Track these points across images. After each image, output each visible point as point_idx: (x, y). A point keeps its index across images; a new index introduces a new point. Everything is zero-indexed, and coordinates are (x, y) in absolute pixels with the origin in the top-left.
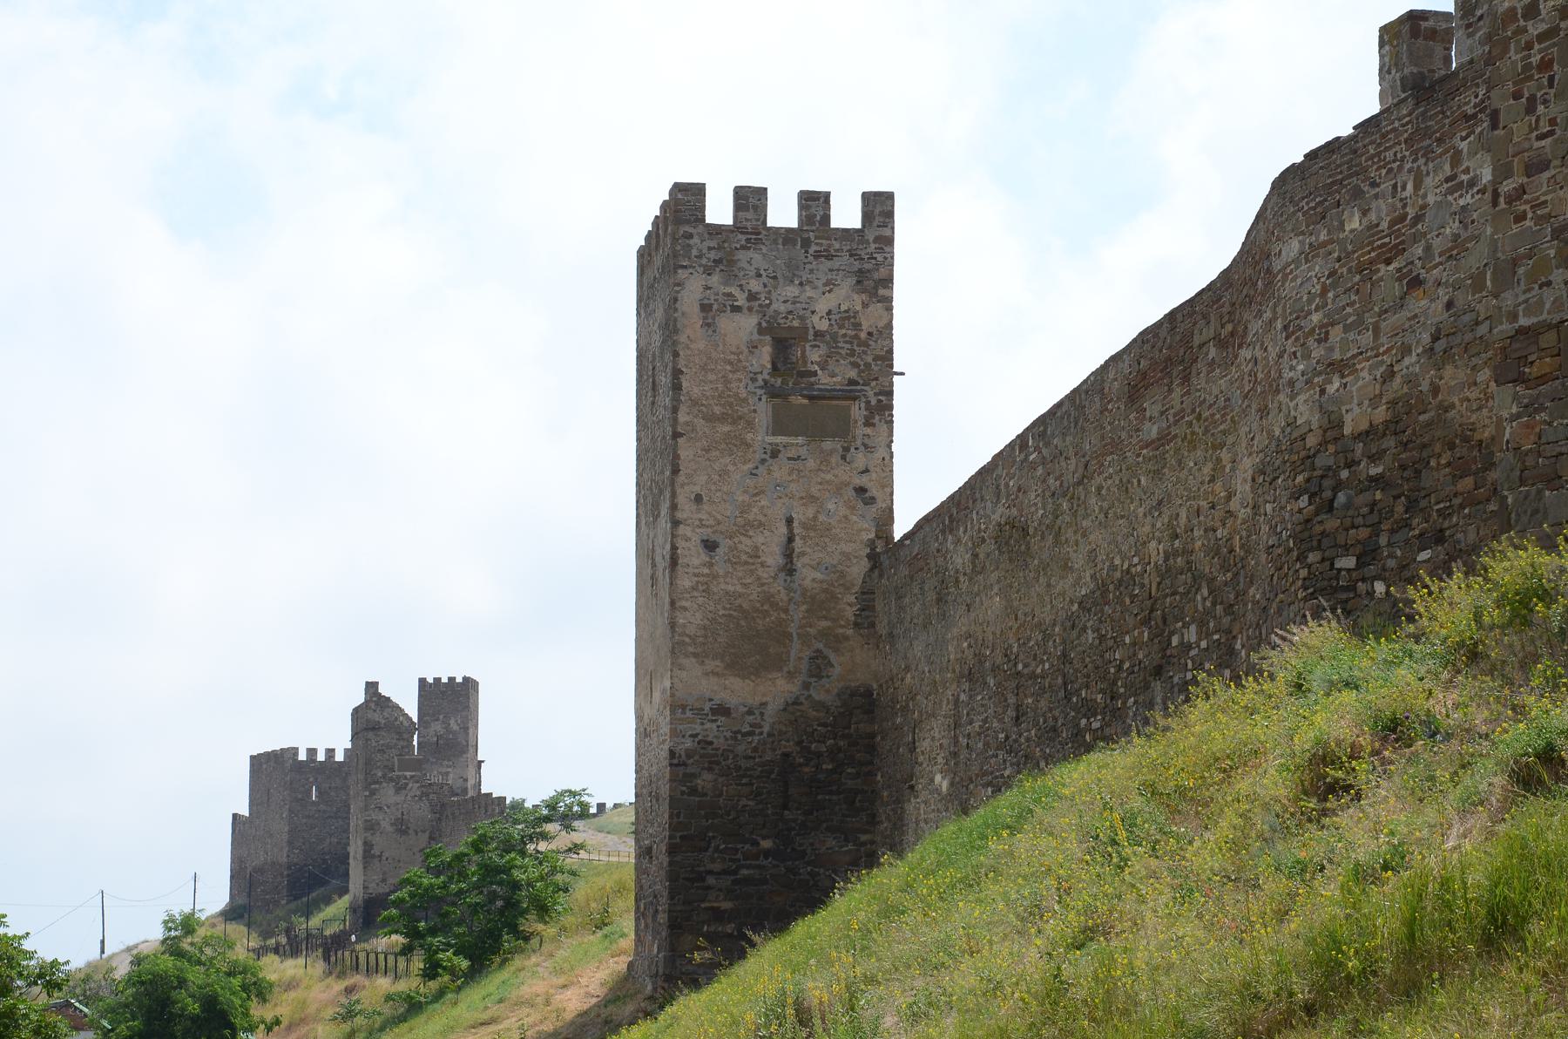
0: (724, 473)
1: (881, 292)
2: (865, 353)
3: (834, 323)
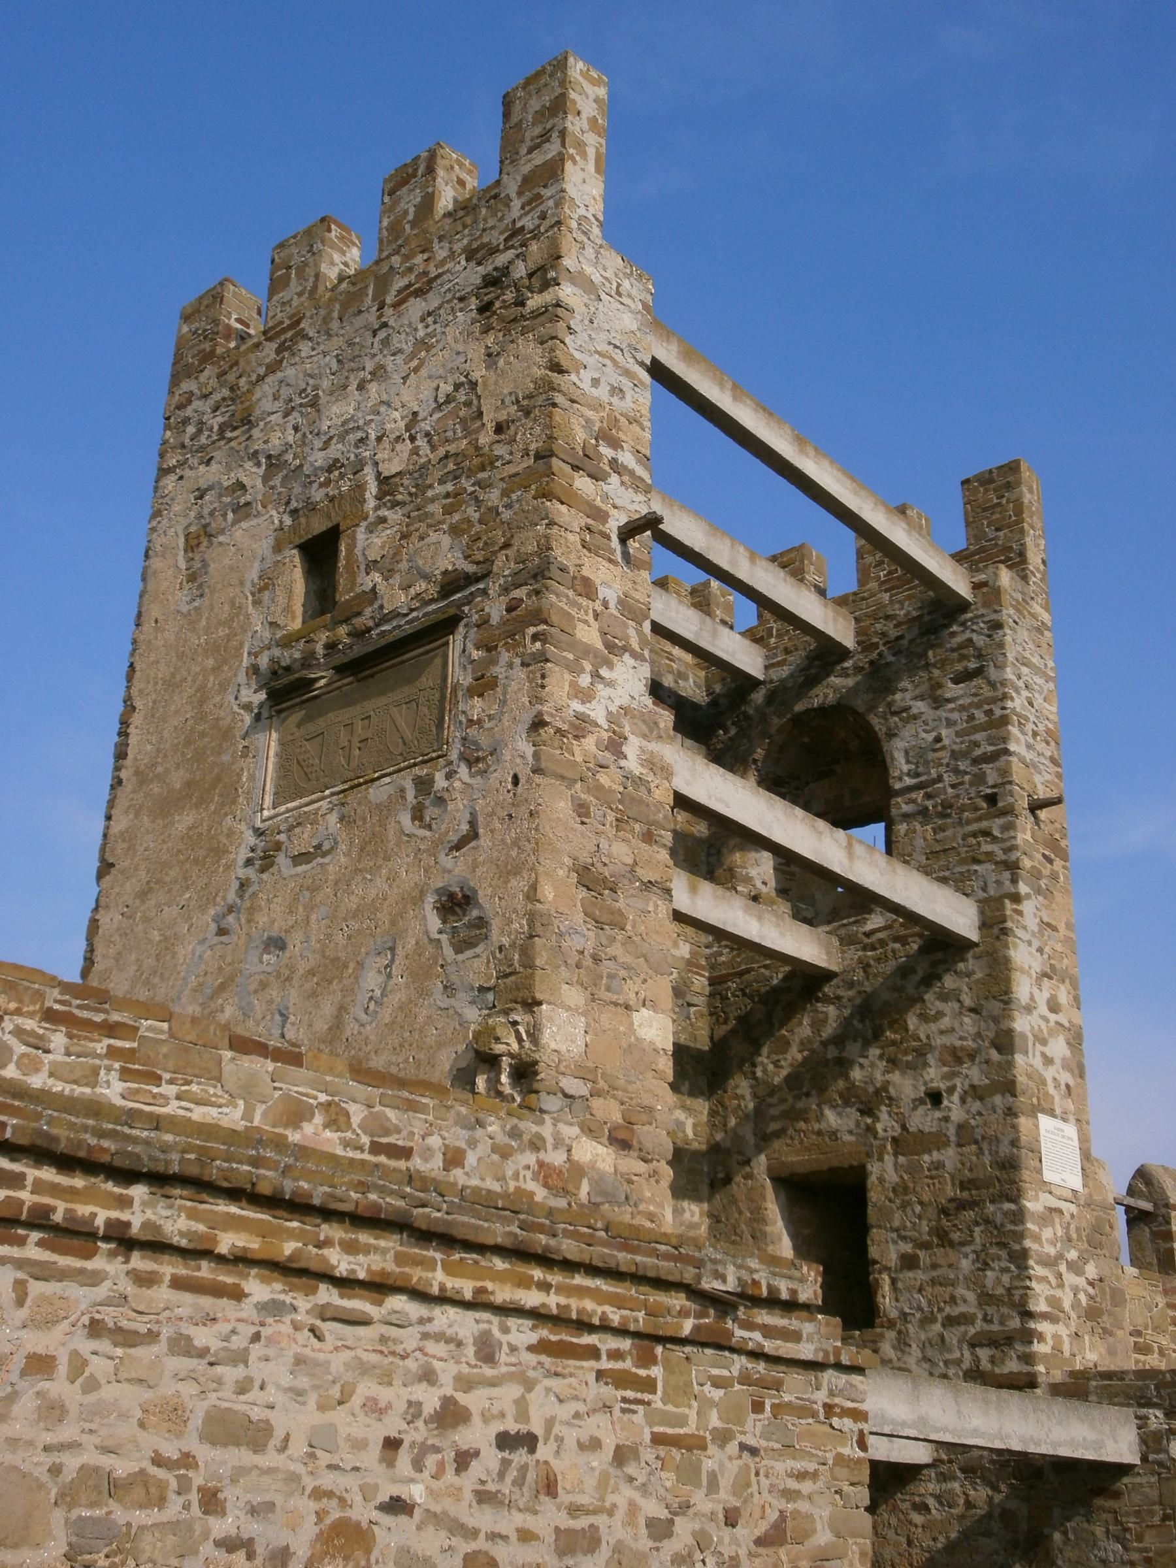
0: (168, 943)
1: (535, 302)
2: (483, 485)
3: (421, 442)
